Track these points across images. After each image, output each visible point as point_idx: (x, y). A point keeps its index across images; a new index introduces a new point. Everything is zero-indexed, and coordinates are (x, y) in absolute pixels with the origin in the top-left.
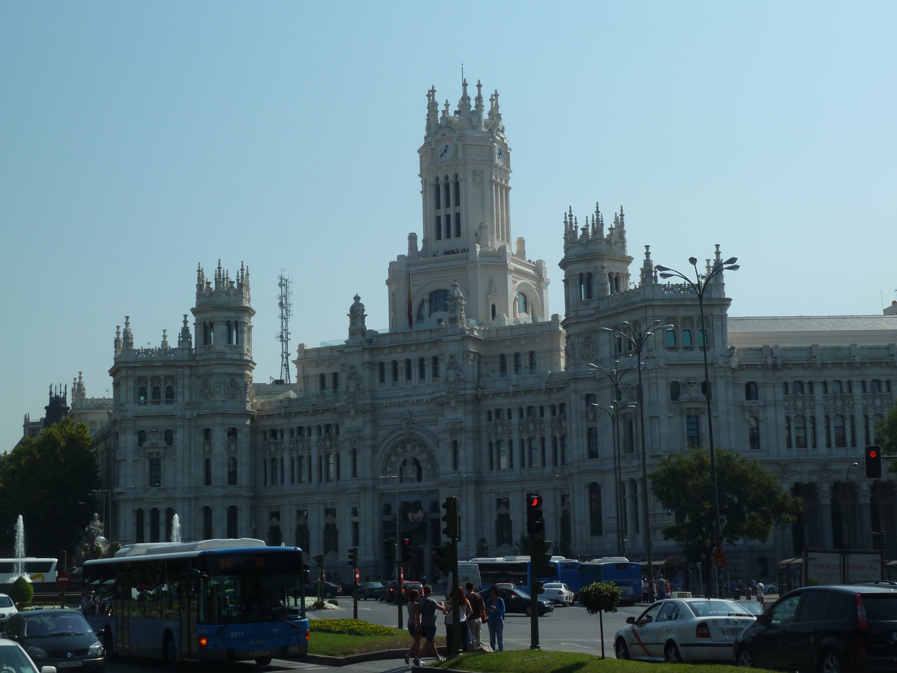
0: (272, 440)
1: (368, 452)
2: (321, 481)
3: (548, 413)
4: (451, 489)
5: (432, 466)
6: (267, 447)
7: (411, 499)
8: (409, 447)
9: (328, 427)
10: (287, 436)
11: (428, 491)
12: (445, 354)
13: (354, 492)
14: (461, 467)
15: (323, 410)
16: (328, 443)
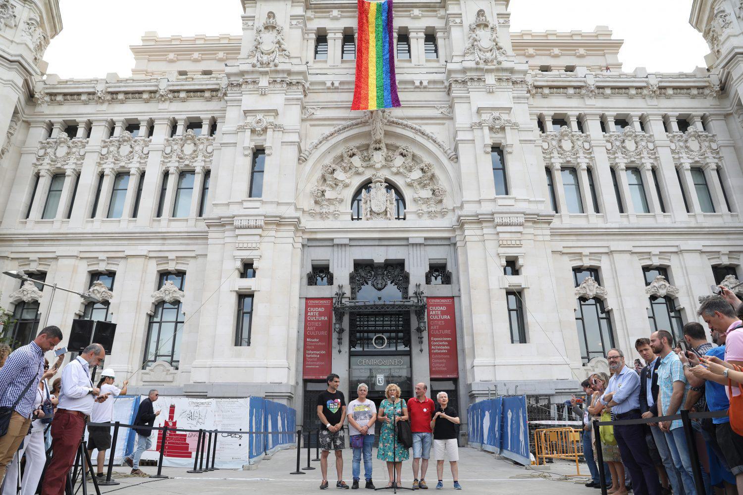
0: (65, 135)
1: (291, 153)
2: (159, 214)
3: (656, 127)
4: (499, 229)
5: (433, 194)
6: (48, 150)
7: (379, 256)
8: (378, 158)
9: (194, 124)
10: (99, 133)
11: (426, 239)
12: (463, 15)
13: (252, 223)
14: (514, 191)
15: (188, 91)
16: (189, 149)
